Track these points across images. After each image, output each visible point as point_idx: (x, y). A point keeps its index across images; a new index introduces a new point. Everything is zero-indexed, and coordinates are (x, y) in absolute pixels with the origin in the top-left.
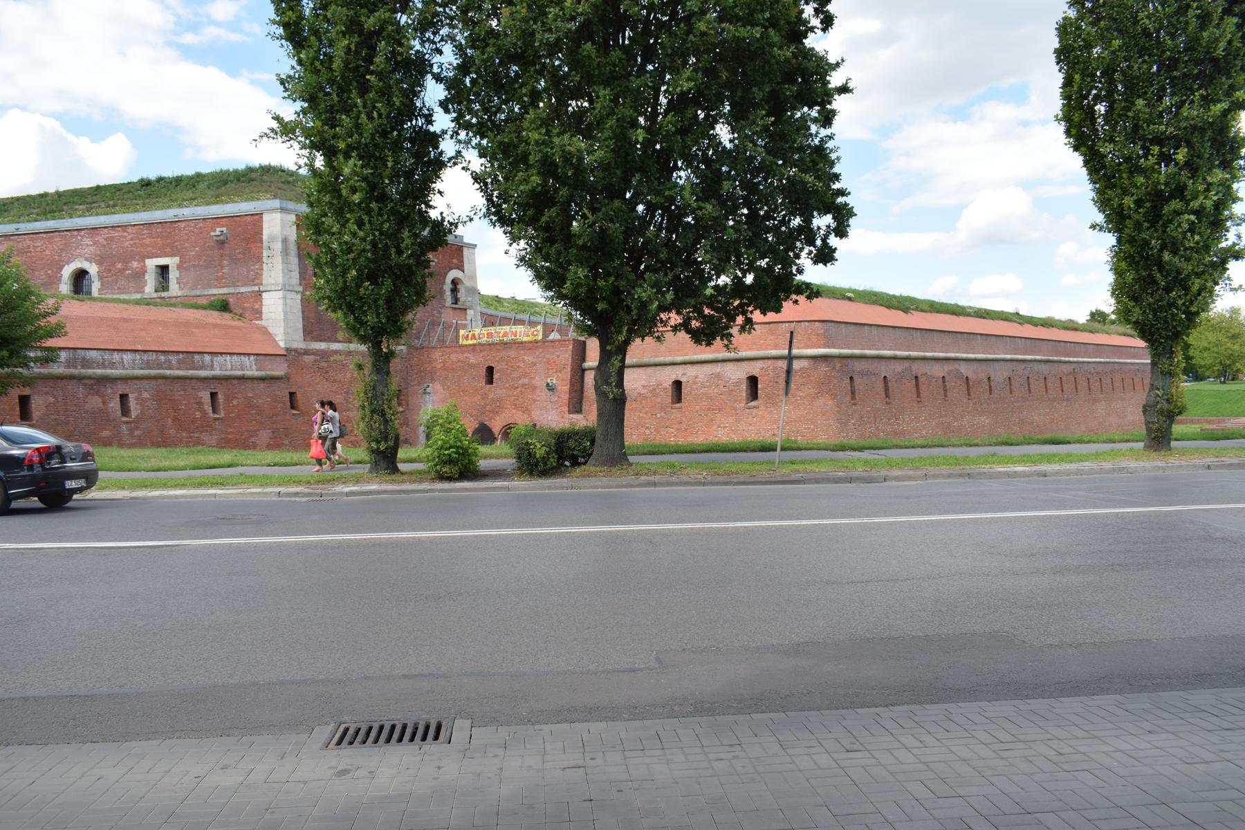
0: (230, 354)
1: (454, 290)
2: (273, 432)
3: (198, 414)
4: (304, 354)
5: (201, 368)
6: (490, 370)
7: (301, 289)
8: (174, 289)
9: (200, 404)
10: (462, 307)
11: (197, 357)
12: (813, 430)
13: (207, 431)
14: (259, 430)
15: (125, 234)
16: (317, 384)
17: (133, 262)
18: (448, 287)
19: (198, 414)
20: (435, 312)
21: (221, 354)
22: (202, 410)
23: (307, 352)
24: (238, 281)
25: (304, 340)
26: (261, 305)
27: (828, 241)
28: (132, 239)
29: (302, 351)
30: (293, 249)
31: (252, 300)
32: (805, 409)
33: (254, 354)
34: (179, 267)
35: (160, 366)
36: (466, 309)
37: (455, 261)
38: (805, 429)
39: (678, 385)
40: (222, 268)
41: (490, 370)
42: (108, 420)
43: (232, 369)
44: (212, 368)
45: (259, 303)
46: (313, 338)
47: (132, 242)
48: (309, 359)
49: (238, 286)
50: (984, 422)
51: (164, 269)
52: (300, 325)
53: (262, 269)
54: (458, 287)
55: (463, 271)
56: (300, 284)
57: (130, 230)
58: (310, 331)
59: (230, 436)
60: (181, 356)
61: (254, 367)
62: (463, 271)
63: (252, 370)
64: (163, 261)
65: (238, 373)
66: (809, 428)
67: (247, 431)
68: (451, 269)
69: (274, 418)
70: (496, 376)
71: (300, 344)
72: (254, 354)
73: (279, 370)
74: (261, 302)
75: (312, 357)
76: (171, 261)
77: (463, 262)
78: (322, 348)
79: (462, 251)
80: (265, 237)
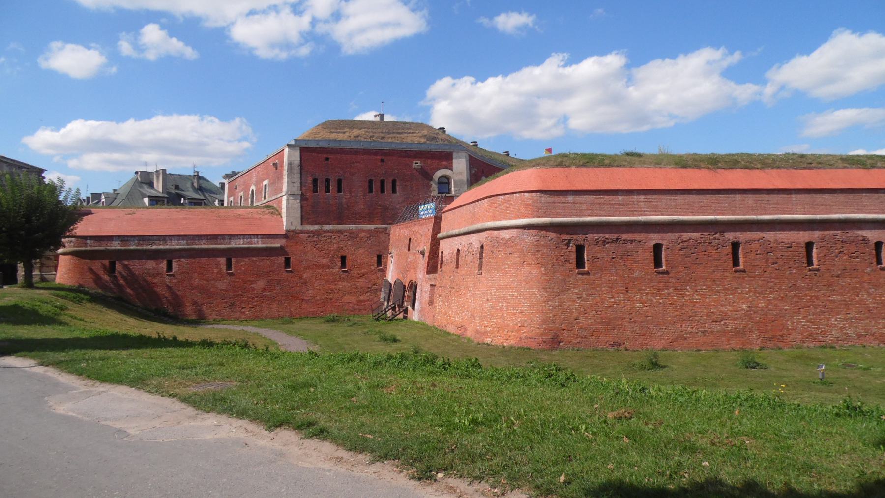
2: (269, 282)
3: (216, 271)
9: (218, 264)
12: (516, 297)
13: (220, 280)
14: (258, 280)
16: (308, 251)
19: (216, 271)
22: (220, 270)
23: (302, 232)
25: (302, 224)
29: (299, 231)
30: (297, 170)
32: (511, 277)
33: (261, 235)
38: (510, 295)
42: (157, 274)
43: (243, 244)
44: (229, 243)
46: (308, 223)
52: (299, 215)
54: (450, 181)
55: (452, 170)
56: (301, 190)
58: (304, 219)
59: (235, 284)
62: (452, 170)
66: (514, 296)
67: (249, 281)
68: (439, 169)
69: (271, 273)
71: (299, 227)
73: (277, 244)
75: (306, 235)
78: (315, 229)
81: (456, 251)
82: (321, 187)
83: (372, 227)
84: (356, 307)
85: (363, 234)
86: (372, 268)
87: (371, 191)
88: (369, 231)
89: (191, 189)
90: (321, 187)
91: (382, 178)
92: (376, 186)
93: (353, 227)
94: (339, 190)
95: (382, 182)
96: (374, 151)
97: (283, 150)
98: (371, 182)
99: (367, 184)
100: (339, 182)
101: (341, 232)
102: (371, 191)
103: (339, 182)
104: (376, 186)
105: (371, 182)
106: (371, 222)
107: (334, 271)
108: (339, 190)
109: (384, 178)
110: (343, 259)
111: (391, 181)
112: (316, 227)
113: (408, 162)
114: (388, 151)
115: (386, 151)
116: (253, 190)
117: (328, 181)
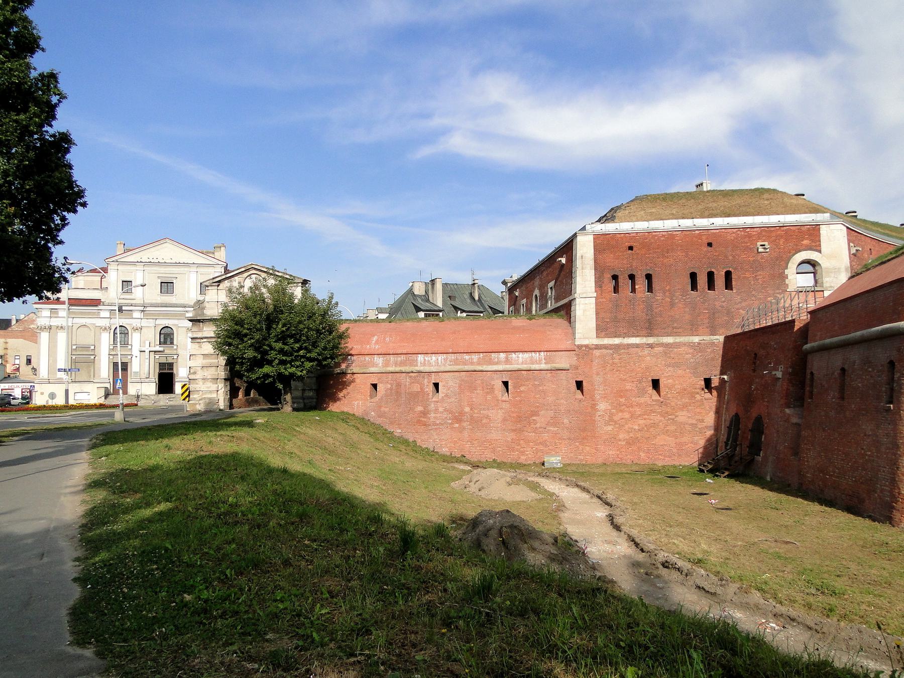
4: (596, 349)
5: (497, 363)
7: (595, 295)
11: (493, 355)
23: (597, 347)
29: (594, 346)
35: (465, 363)
37: (805, 242)
48: (597, 353)
55: (820, 251)
56: (596, 291)
58: (602, 330)
62: (820, 251)
65: (525, 367)
72: (544, 351)
77: (820, 241)
78: (615, 343)
81: (839, 372)
82: (625, 283)
83: (696, 339)
84: (675, 451)
86: (698, 397)
87: (694, 287)
88: (691, 345)
89: (469, 301)
90: (625, 283)
91: (709, 270)
92: (702, 281)
93: (670, 340)
94: (650, 289)
95: (711, 275)
96: (697, 232)
98: (693, 276)
99: (688, 281)
100: (649, 277)
101: (651, 346)
102: (694, 287)
103: (649, 277)
104: (702, 281)
105: (693, 276)
106: (694, 331)
107: (642, 400)
108: (650, 289)
110: (656, 384)
111: (723, 273)
112: (617, 341)
113: (749, 244)
115: (715, 231)
116: (536, 295)
117: (632, 277)
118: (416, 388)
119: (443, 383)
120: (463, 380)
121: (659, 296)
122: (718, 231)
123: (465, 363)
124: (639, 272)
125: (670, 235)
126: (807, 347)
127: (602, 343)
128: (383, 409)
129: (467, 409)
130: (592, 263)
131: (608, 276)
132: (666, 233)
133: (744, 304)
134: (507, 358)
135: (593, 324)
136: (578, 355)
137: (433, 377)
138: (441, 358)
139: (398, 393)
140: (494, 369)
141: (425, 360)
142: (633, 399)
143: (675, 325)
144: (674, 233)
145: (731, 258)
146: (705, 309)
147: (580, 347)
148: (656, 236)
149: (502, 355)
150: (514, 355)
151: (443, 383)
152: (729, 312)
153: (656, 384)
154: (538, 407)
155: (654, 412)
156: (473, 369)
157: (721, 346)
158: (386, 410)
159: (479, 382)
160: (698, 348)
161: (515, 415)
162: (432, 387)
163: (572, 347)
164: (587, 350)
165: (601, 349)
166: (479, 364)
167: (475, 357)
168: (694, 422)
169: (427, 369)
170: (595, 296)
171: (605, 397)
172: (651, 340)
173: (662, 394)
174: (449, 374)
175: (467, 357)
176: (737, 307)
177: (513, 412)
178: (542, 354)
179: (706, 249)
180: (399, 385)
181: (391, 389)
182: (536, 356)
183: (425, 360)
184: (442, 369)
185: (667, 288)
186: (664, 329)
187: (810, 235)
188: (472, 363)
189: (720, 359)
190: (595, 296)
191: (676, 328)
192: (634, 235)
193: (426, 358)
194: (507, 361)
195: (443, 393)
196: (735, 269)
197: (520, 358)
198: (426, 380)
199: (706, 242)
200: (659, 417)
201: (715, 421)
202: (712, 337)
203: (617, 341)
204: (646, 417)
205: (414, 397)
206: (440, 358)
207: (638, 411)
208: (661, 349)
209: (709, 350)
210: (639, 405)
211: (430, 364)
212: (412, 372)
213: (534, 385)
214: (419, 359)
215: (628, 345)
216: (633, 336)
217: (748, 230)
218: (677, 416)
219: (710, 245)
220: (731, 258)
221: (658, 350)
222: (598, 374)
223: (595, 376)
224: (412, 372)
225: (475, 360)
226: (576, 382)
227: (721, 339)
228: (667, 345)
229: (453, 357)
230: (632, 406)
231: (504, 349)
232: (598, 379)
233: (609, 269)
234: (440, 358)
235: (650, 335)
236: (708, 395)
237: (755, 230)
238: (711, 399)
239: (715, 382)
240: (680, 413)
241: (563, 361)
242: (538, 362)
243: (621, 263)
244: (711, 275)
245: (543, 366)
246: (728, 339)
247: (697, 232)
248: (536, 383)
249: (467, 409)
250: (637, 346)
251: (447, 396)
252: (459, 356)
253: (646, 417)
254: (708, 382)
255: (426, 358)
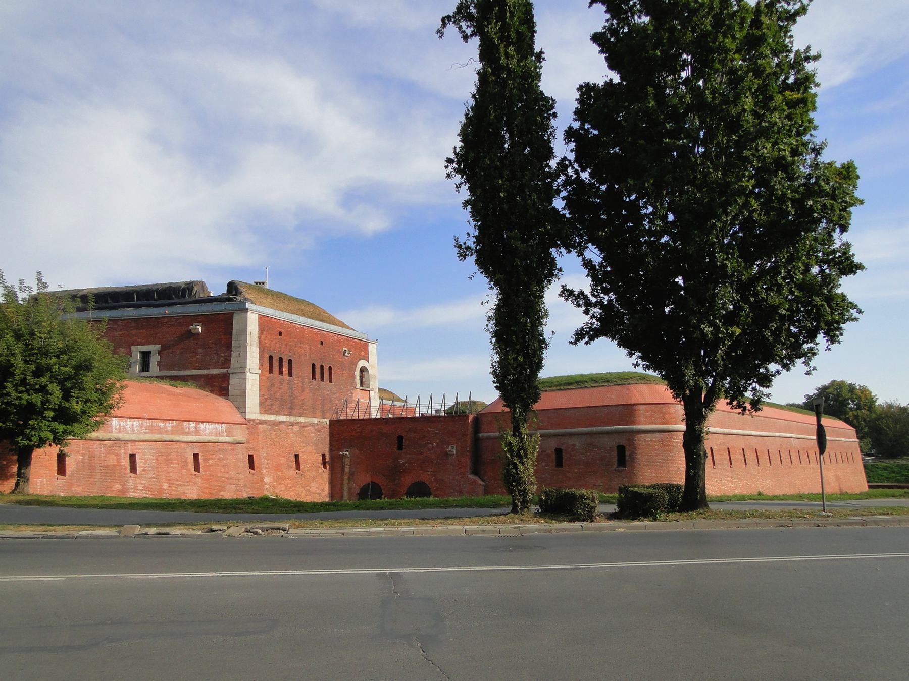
0: (208, 422)
1: (361, 377)
4: (260, 424)
5: (188, 434)
6: (400, 439)
7: (259, 372)
8: (154, 369)
10: (367, 389)
11: (185, 424)
15: (116, 326)
17: (121, 348)
18: (357, 373)
20: (349, 393)
21: (203, 422)
23: (262, 422)
24: (209, 365)
26: (229, 384)
27: (837, 342)
28: (121, 331)
31: (220, 380)
34: (160, 353)
35: (160, 431)
36: (369, 391)
37: (363, 353)
39: (559, 452)
40: (197, 354)
41: (400, 439)
45: (227, 382)
47: (120, 333)
48: (261, 427)
49: (209, 369)
50: (769, 484)
51: (146, 356)
53: (231, 356)
57: (120, 324)
58: (264, 407)
60: (175, 423)
61: (225, 434)
63: (223, 436)
64: (146, 348)
65: (213, 438)
68: (360, 360)
70: (405, 443)
74: (229, 382)
76: (154, 348)
78: (272, 419)
79: (368, 346)
80: (234, 332)
83: (316, 421)
85: (310, 429)
87: (314, 377)
93: (302, 420)
94: (290, 374)
95: (322, 367)
97: (233, 313)
98: (313, 365)
101: (292, 424)
103: (290, 361)
108: (290, 374)
109: (323, 364)
114: (325, 333)
118: (112, 460)
119: (141, 455)
120: (159, 452)
121: (296, 379)
122: (325, 333)
123: (160, 431)
124: (285, 357)
125: (302, 329)
126: (481, 435)
127: (263, 419)
128: (75, 488)
129: (165, 486)
130: (257, 340)
131: (267, 356)
132: (299, 326)
133: (337, 395)
134: (196, 428)
135: (257, 400)
136: (248, 429)
137: (130, 447)
138: (136, 423)
139: (92, 468)
140: (186, 440)
141: (120, 425)
142: (286, 472)
143: (304, 407)
144: (305, 328)
145: (331, 356)
146: (320, 396)
147: (250, 420)
148: (294, 327)
149: (192, 425)
150: (201, 426)
151: (141, 455)
152: (331, 401)
153: (297, 456)
154: (223, 482)
155: (298, 484)
156: (171, 439)
157: (328, 427)
158: (79, 489)
159: (174, 454)
160: (317, 427)
161: (206, 491)
162: (126, 462)
163: (244, 421)
164: (254, 424)
165: (263, 424)
166: (173, 433)
167: (169, 425)
168: (319, 491)
169: (127, 437)
170: (260, 373)
171: (269, 471)
172: (292, 419)
173: (301, 467)
174: (146, 443)
175: (161, 425)
176: (335, 396)
177: (205, 488)
178: (223, 425)
179: (320, 346)
180: (92, 456)
181: (83, 462)
182: (218, 426)
183: (120, 425)
184: (142, 437)
185: (300, 374)
186: (299, 410)
187: (364, 348)
188: (167, 433)
189: (328, 438)
190: (260, 373)
191: (304, 410)
192: (282, 322)
193: (121, 423)
194: (197, 432)
195: (141, 467)
196: (334, 366)
197: (207, 430)
198: (122, 451)
199: (320, 340)
200: (301, 489)
201: (329, 490)
202: (323, 419)
203: (272, 418)
204: (294, 489)
205: (110, 471)
206: (135, 424)
207: (289, 483)
208: (298, 427)
209: (322, 431)
210: (289, 478)
211: (125, 431)
212: (109, 440)
213: (219, 459)
214: (113, 423)
215: (279, 422)
216: (282, 414)
217: (339, 336)
218: (310, 487)
219: (322, 343)
220: (331, 356)
221: (297, 428)
222: (263, 449)
223: (261, 450)
224: (109, 440)
225: (169, 429)
226: (249, 455)
227: (328, 421)
228: (301, 424)
229: (147, 423)
230: (285, 479)
231: (193, 418)
232: (263, 454)
233: (267, 349)
234: (135, 424)
235: (291, 415)
236: (325, 470)
237: (342, 337)
238: (325, 474)
239: (327, 459)
240: (313, 485)
241: (240, 435)
242: (221, 434)
243: (277, 348)
244: (322, 367)
245: (228, 439)
246: (330, 421)
247: (316, 330)
248: (221, 456)
249: (165, 486)
250: (284, 423)
251: (144, 470)
252: (154, 423)
253: (294, 489)
254: (323, 456)
255: (121, 423)
